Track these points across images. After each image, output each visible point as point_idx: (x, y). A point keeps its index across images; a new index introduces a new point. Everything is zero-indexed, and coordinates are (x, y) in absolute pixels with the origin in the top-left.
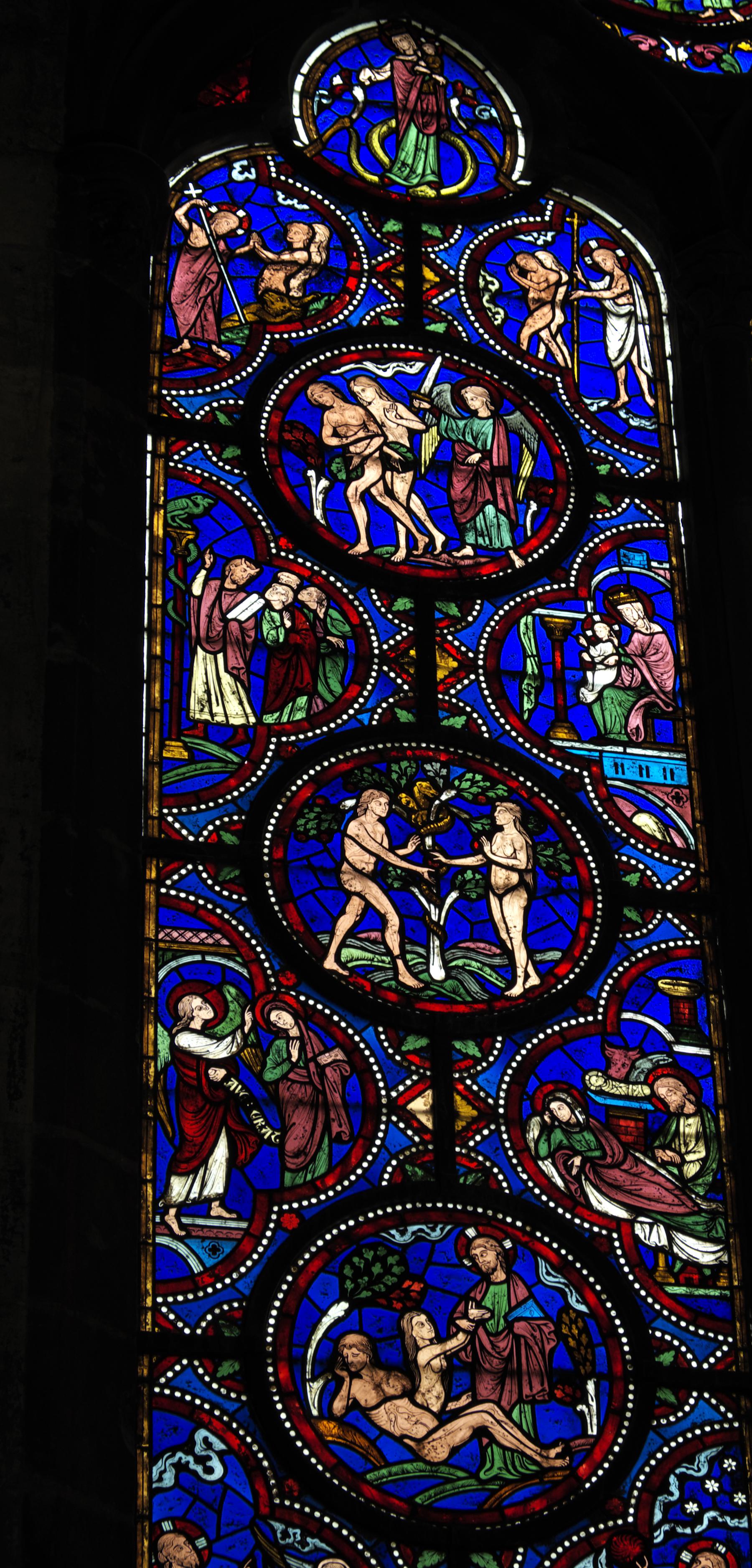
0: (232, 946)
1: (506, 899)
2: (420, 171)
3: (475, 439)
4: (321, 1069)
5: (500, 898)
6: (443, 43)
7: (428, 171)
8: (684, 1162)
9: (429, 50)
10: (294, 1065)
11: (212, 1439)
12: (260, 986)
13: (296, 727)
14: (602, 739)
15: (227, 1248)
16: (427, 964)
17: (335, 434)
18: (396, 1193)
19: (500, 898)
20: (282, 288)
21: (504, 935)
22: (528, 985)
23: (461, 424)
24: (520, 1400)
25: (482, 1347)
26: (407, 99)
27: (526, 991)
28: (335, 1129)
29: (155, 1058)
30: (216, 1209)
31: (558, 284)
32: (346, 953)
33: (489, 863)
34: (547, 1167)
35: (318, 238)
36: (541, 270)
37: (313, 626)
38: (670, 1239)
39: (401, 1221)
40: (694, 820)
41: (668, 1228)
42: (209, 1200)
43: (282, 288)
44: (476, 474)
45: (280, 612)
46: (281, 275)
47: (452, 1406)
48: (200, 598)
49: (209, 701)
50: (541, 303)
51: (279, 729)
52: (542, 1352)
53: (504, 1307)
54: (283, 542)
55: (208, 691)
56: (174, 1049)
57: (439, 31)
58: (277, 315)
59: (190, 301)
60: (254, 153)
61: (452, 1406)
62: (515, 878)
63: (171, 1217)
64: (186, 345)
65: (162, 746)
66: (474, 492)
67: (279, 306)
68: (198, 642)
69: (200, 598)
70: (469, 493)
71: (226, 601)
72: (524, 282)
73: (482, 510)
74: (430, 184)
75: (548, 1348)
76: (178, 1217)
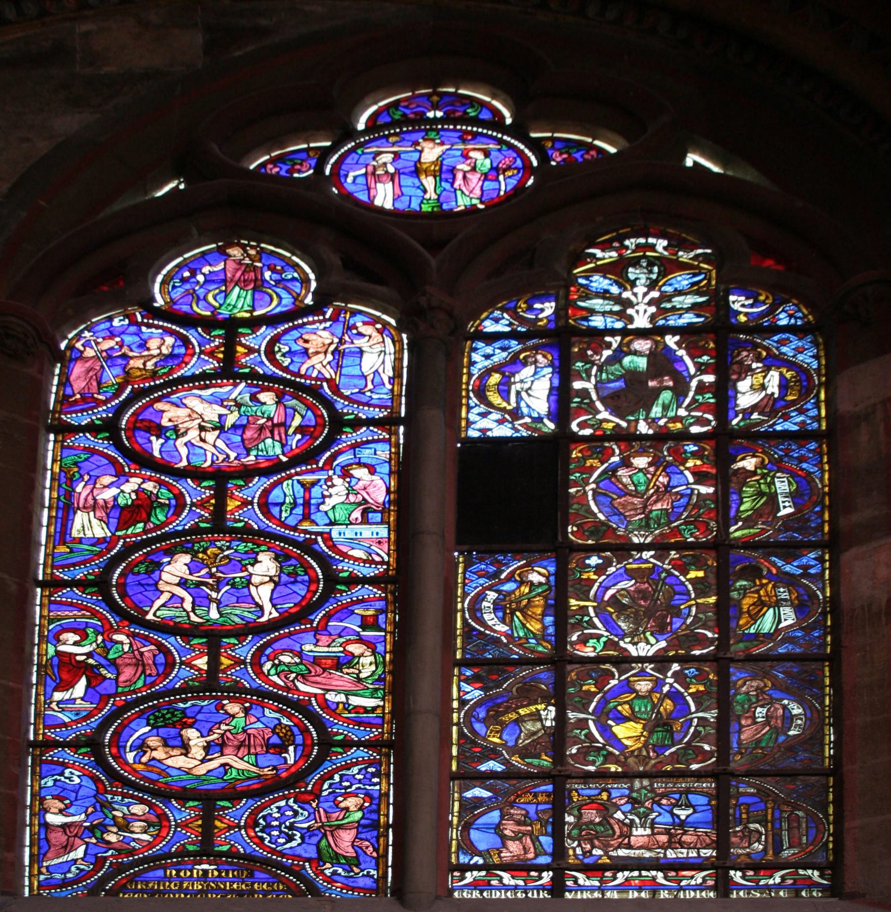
0: (92, 614)
1: (259, 588)
2: (240, 306)
3: (263, 414)
4: (142, 654)
5: (257, 587)
6: (262, 248)
7: (246, 305)
8: (360, 672)
9: (252, 252)
10: (125, 653)
11: (74, 771)
12: (107, 627)
13: (136, 535)
14: (332, 523)
15: (84, 714)
16: (208, 611)
17: (170, 420)
18: (182, 690)
19: (257, 587)
20: (142, 366)
21: (257, 600)
22: (271, 617)
23: (254, 409)
24: (249, 754)
25: (228, 738)
26: (234, 276)
27: (269, 620)
28: (148, 672)
29: (46, 654)
30: (78, 701)
31: (332, 343)
32: (158, 613)
33: (251, 575)
34: (275, 679)
35: (166, 343)
36: (320, 339)
37: (149, 497)
38: (347, 699)
39: (184, 701)
40: (389, 550)
41: (346, 695)
42: (75, 699)
43: (142, 366)
44: (262, 428)
45: (130, 494)
46: (142, 361)
47: (208, 757)
48: (80, 493)
49: (84, 530)
50: (317, 353)
51: (126, 536)
52: (263, 739)
53: (243, 724)
54: (133, 466)
55: (83, 527)
56: (57, 652)
57: (259, 242)
58: (137, 377)
59: (82, 379)
60: (127, 313)
61: (208, 757)
62: (267, 579)
63: (54, 705)
64: (78, 396)
65: (54, 548)
66: (260, 435)
67: (139, 373)
68: (79, 508)
69: (80, 493)
70: (256, 435)
71: (95, 492)
72: (306, 345)
73: (263, 441)
74: (246, 311)
75: (266, 737)
76: (57, 705)
